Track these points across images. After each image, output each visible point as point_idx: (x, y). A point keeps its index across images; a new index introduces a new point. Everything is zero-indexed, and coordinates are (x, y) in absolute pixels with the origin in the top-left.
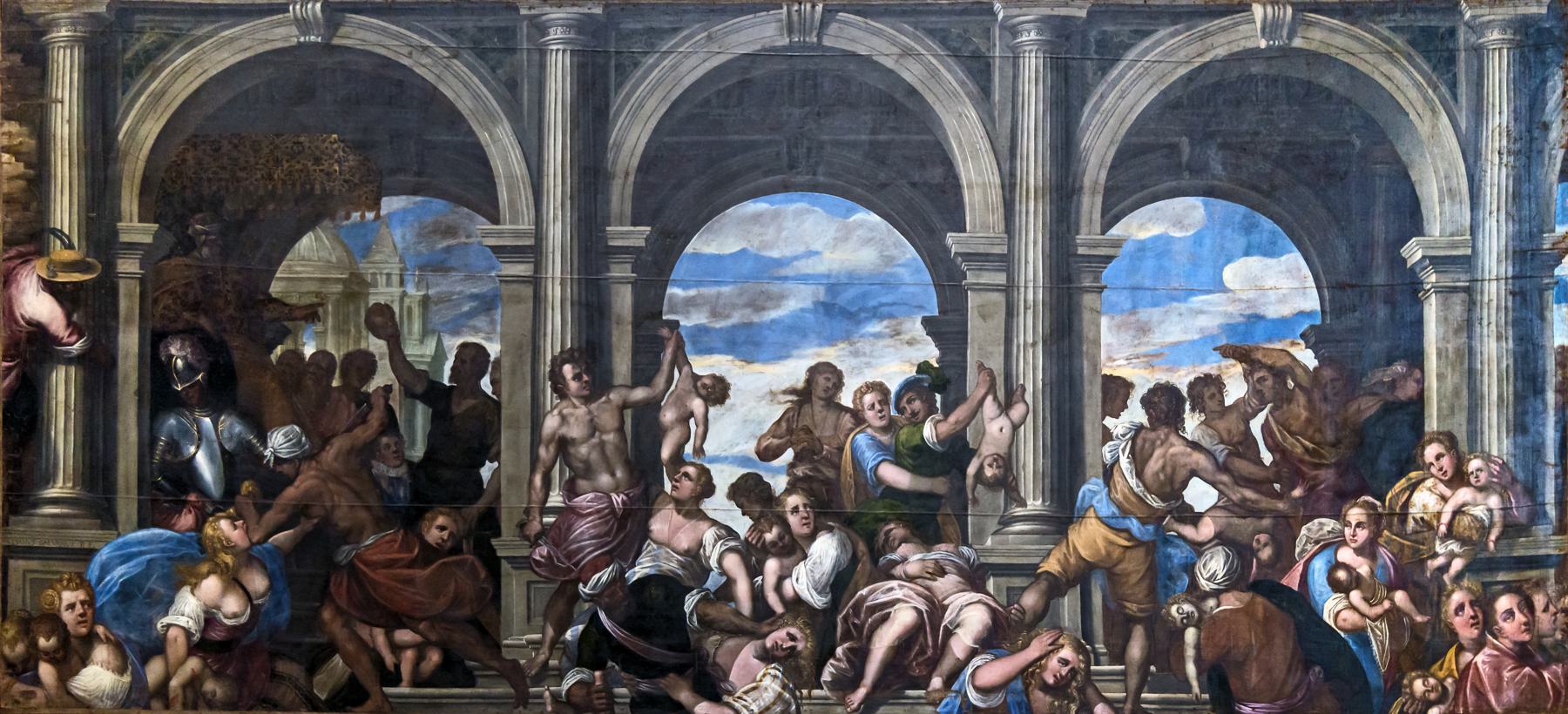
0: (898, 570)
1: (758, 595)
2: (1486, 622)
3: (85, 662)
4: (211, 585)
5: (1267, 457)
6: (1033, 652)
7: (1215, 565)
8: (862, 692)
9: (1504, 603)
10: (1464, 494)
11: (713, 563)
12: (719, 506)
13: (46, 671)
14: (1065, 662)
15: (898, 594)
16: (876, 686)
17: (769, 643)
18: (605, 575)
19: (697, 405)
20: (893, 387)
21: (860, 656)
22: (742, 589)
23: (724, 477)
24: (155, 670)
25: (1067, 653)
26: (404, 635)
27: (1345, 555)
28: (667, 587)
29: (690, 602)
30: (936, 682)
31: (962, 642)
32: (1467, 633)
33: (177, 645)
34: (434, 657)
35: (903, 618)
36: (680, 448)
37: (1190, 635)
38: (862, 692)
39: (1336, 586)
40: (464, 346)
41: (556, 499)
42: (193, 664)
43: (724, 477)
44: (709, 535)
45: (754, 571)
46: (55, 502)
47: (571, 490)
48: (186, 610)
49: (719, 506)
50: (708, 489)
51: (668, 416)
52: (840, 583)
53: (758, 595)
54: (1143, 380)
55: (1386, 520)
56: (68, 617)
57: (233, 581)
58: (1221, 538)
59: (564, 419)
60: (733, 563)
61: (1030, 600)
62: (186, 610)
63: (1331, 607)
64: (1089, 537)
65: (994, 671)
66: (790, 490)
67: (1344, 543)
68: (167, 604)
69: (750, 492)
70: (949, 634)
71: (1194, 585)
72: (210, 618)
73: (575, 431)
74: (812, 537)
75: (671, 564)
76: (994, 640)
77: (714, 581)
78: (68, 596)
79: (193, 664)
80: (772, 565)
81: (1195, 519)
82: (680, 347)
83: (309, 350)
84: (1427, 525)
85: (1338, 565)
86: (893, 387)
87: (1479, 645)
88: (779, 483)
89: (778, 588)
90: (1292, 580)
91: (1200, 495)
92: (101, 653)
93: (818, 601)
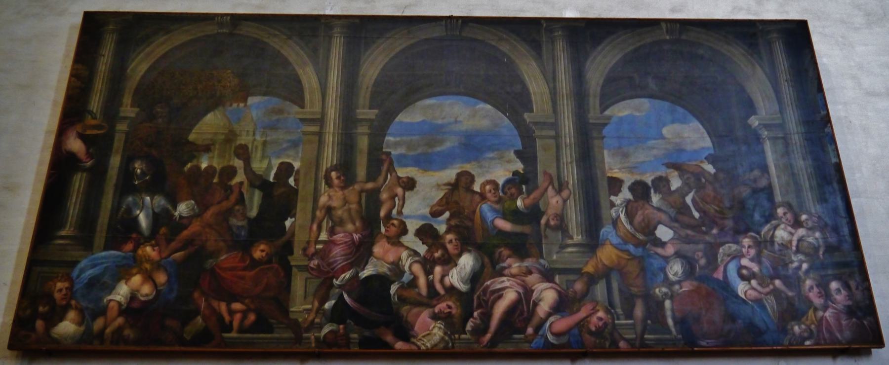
0: (506, 272)
1: (430, 285)
2: (826, 294)
3: (61, 319)
4: (137, 279)
5: (696, 215)
6: (582, 314)
7: (676, 269)
8: (488, 336)
9: (834, 285)
10: (801, 232)
11: (406, 268)
12: (410, 239)
13: (39, 324)
14: (600, 319)
15: (507, 284)
16: (496, 333)
17: (436, 310)
18: (347, 275)
19: (399, 191)
20: (501, 182)
21: (487, 316)
22: (422, 281)
23: (412, 226)
24: (99, 324)
25: (601, 314)
26: (237, 306)
27: (745, 262)
28: (381, 282)
29: (393, 289)
30: (530, 330)
31: (543, 308)
32: (818, 301)
33: (113, 309)
34: (252, 317)
35: (510, 296)
36: (390, 212)
37: (668, 304)
38: (488, 336)
39: (743, 278)
40: (282, 163)
41: (324, 236)
42: (120, 320)
43: (412, 226)
44: (405, 254)
45: (428, 272)
46: (62, 238)
47: (332, 232)
48: (122, 292)
49: (410, 239)
50: (404, 231)
51: (384, 196)
52: (475, 279)
53: (430, 285)
54: (628, 179)
55: (763, 244)
56: (57, 296)
57: (149, 277)
58: (678, 255)
59: (330, 197)
60: (417, 268)
61: (579, 286)
62: (122, 292)
63: (741, 288)
64: (607, 254)
65: (561, 323)
66: (448, 231)
67: (743, 256)
68: (111, 289)
69: (426, 233)
70: (536, 304)
71: (666, 277)
72: (133, 297)
73: (335, 203)
74: (460, 255)
75: (384, 269)
76: (562, 306)
77: (406, 278)
78: (59, 285)
79: (120, 320)
80: (438, 270)
81: (662, 244)
82: (391, 163)
83: (204, 165)
84: (785, 246)
85: (741, 268)
86: (501, 182)
87: (825, 308)
88: (442, 228)
89: (442, 281)
90: (719, 275)
91: (664, 233)
92: (72, 314)
93: (463, 287)
